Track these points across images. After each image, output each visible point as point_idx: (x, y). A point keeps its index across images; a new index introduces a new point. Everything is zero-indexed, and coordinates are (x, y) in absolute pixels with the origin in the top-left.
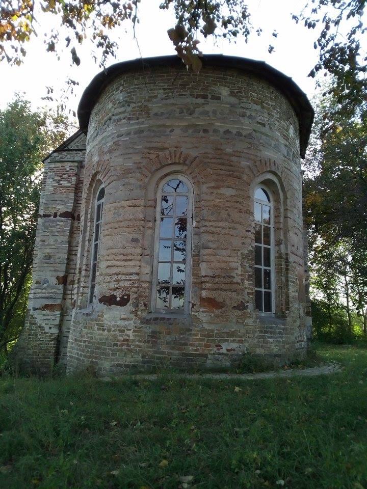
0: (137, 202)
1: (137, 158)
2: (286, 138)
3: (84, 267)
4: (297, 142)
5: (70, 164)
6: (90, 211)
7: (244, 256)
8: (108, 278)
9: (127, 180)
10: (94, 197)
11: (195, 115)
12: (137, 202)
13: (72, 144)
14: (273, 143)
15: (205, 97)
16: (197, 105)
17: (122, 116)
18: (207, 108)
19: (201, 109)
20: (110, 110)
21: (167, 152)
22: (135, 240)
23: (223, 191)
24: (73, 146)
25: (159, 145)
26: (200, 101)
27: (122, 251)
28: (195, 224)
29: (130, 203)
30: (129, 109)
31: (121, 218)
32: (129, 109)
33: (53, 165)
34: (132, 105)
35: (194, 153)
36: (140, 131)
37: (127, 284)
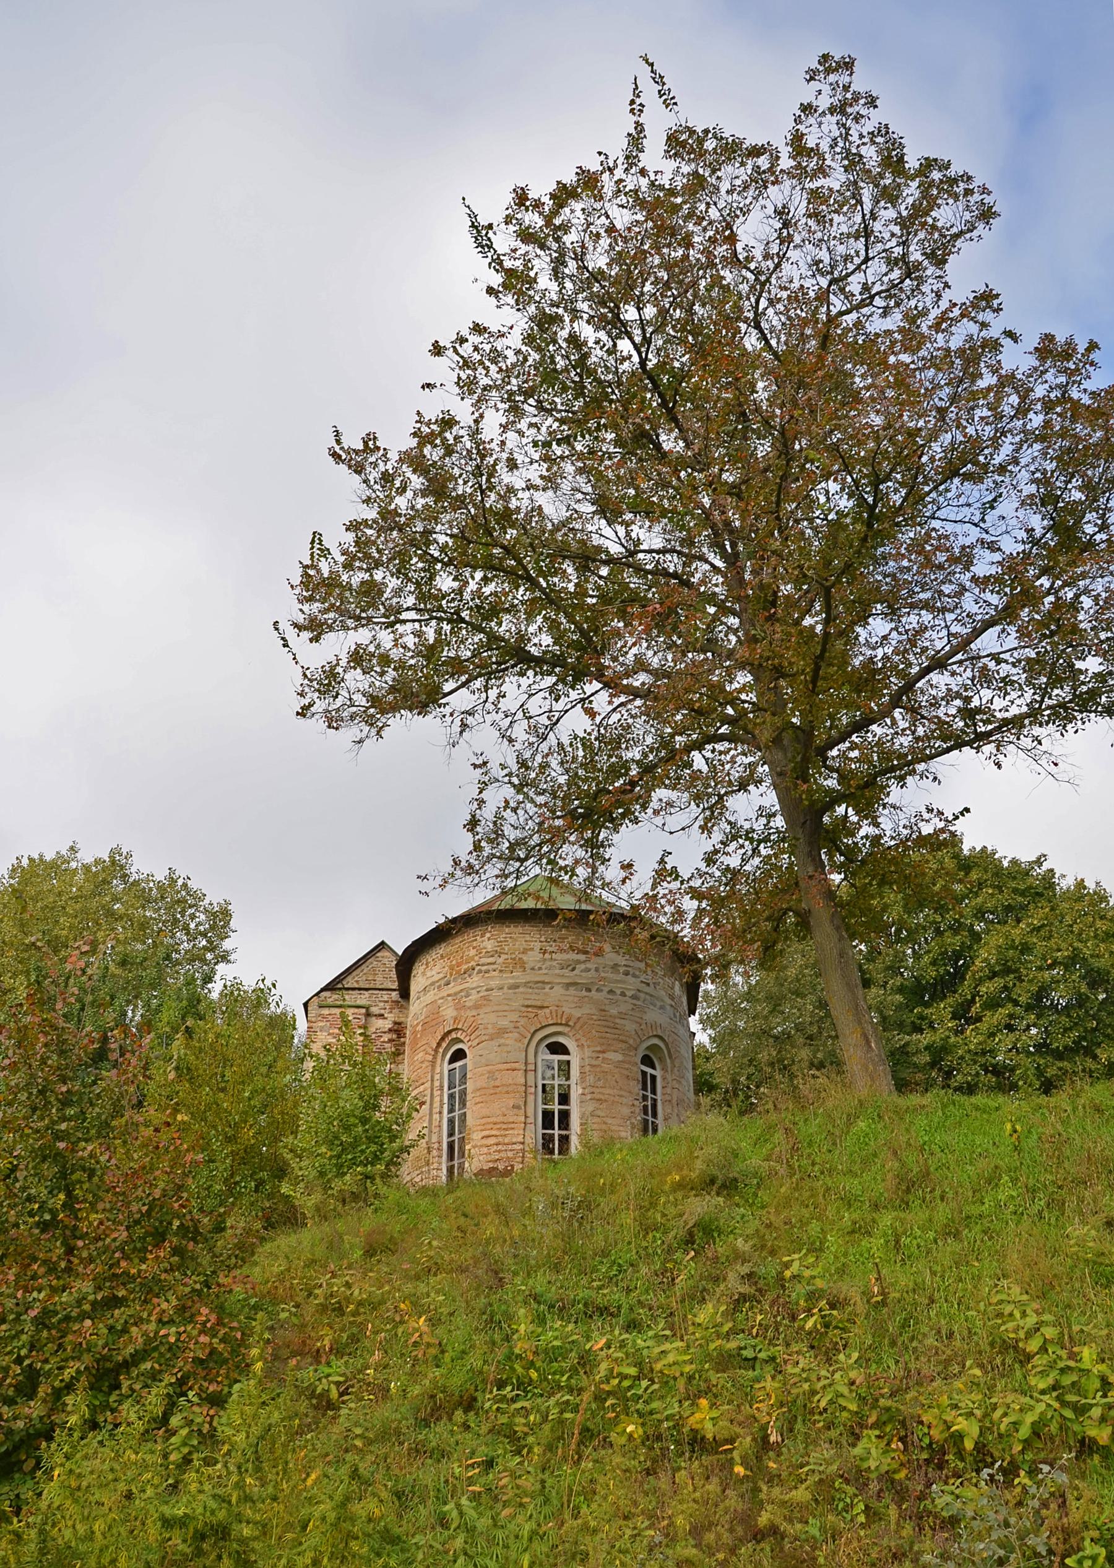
0: (516, 1065)
1: (514, 1017)
2: (672, 997)
3: (436, 1146)
4: (684, 999)
5: (352, 1010)
6: (437, 1077)
7: (633, 1127)
8: (485, 1150)
9: (502, 1041)
10: (443, 1060)
11: (576, 972)
12: (516, 1065)
13: (349, 978)
14: (659, 1004)
15: (586, 953)
16: (579, 962)
17: (491, 967)
18: (588, 965)
19: (583, 966)
20: (472, 958)
21: (547, 1011)
22: (519, 1107)
23: (611, 1055)
24: (350, 982)
25: (539, 1004)
26: (582, 957)
27: (501, 1119)
28: (580, 1091)
29: (508, 1066)
30: (500, 960)
31: (498, 1083)
32: (500, 960)
33: (326, 1011)
34: (504, 957)
35: (577, 1013)
36: (515, 987)
37: (510, 1154)
